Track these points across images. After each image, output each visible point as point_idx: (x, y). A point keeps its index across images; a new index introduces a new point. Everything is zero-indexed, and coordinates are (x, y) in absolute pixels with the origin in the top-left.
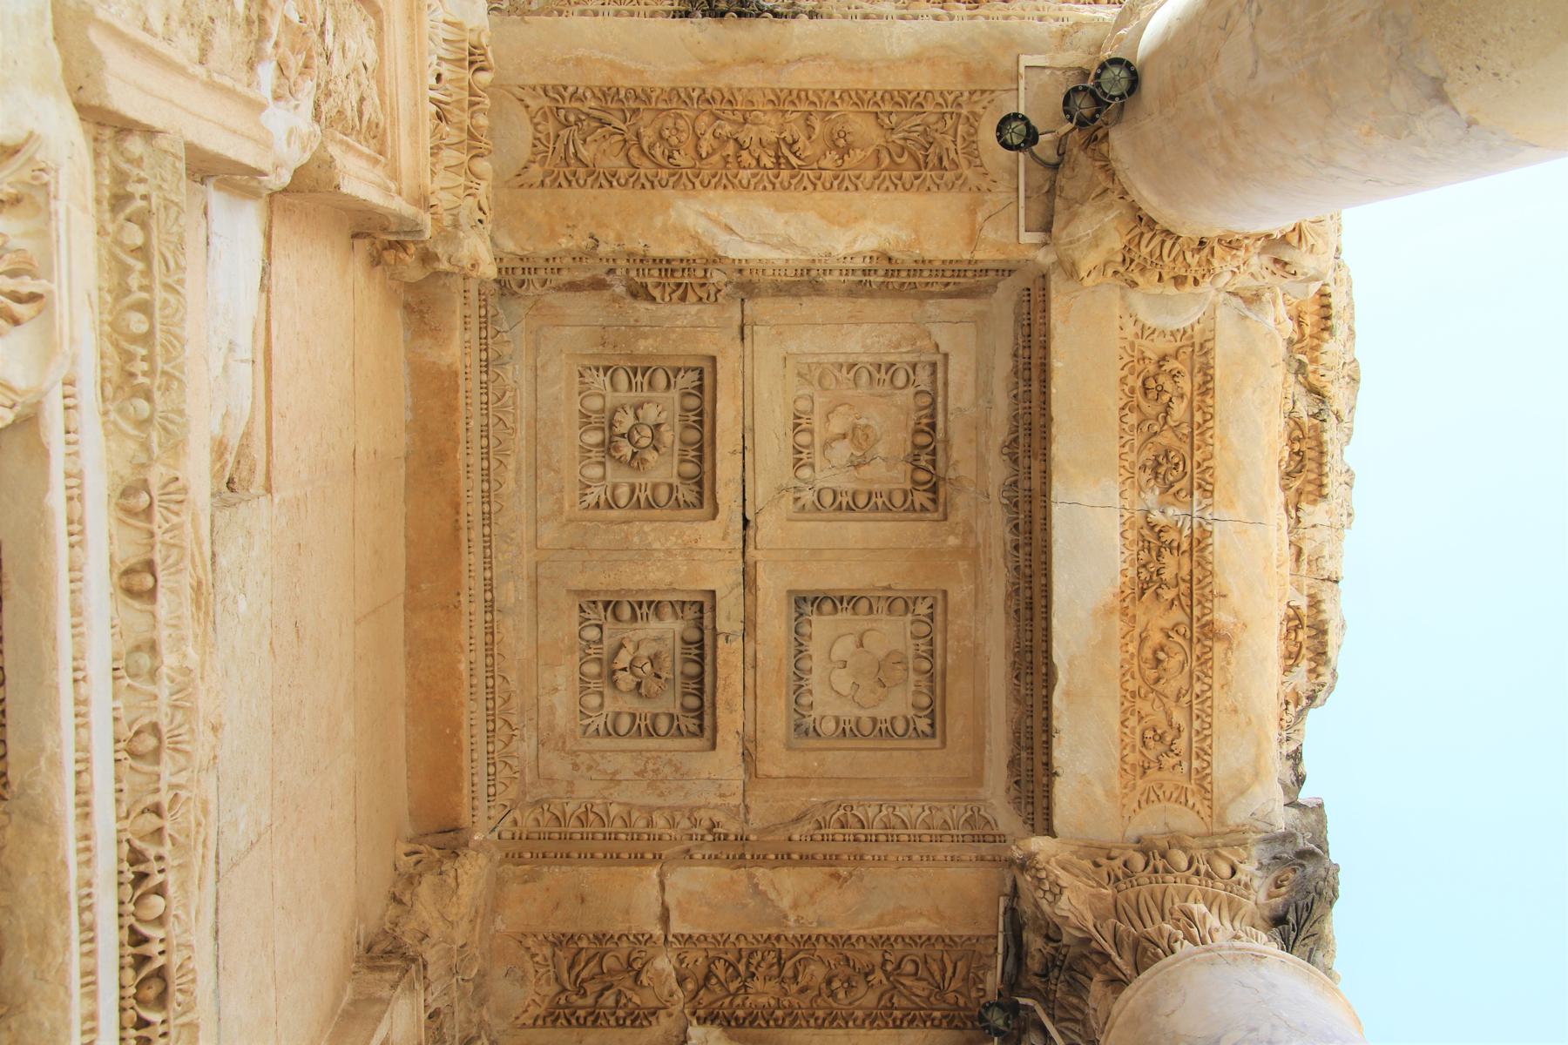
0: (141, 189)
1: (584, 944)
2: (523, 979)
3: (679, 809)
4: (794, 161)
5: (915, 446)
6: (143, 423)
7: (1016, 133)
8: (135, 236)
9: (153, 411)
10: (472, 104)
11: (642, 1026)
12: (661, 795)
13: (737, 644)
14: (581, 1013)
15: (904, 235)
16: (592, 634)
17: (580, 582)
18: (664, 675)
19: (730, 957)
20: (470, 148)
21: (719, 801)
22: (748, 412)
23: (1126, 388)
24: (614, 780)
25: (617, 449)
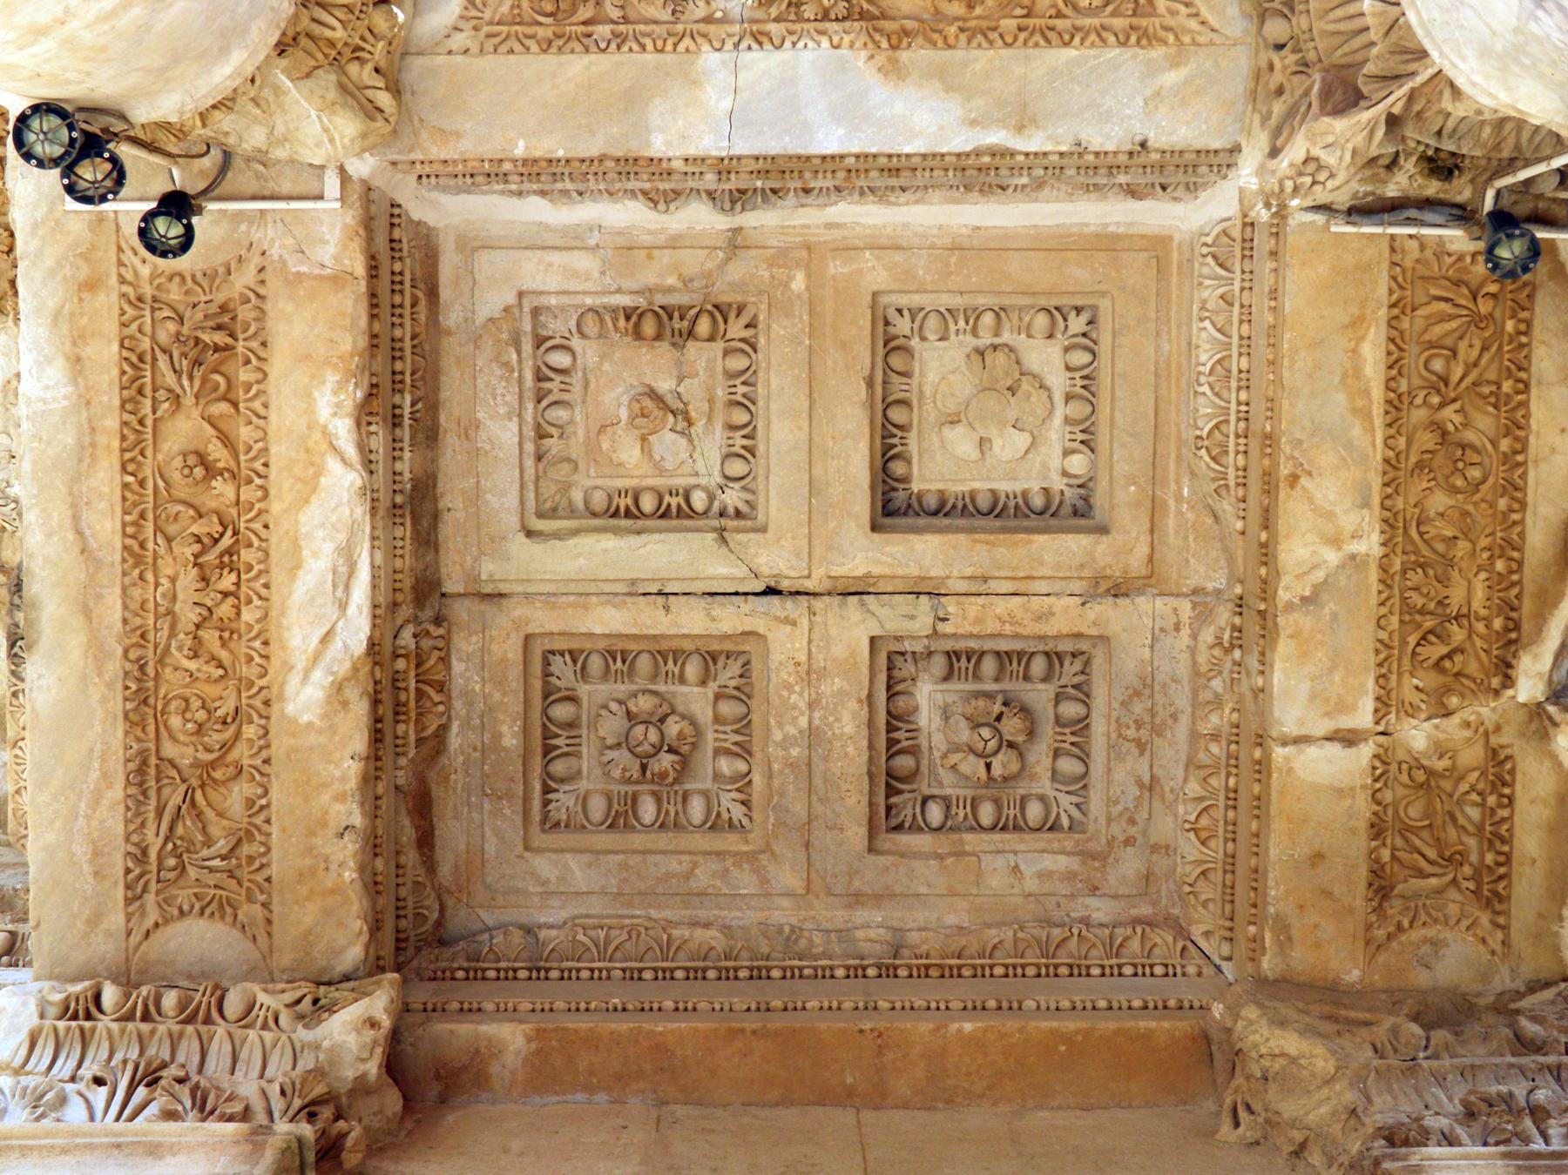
1: (1386, 855)
2: (1436, 944)
3: (1195, 693)
4: (227, 541)
5: (658, 337)
7: (167, 229)
10: (146, 1017)
11: (1512, 772)
13: (951, 605)
14: (1490, 858)
15: (332, 378)
16: (935, 813)
17: (857, 834)
19: (1412, 640)
20: (208, 1021)
21: (1185, 632)
22: (608, 588)
24: (1151, 786)
25: (663, 775)
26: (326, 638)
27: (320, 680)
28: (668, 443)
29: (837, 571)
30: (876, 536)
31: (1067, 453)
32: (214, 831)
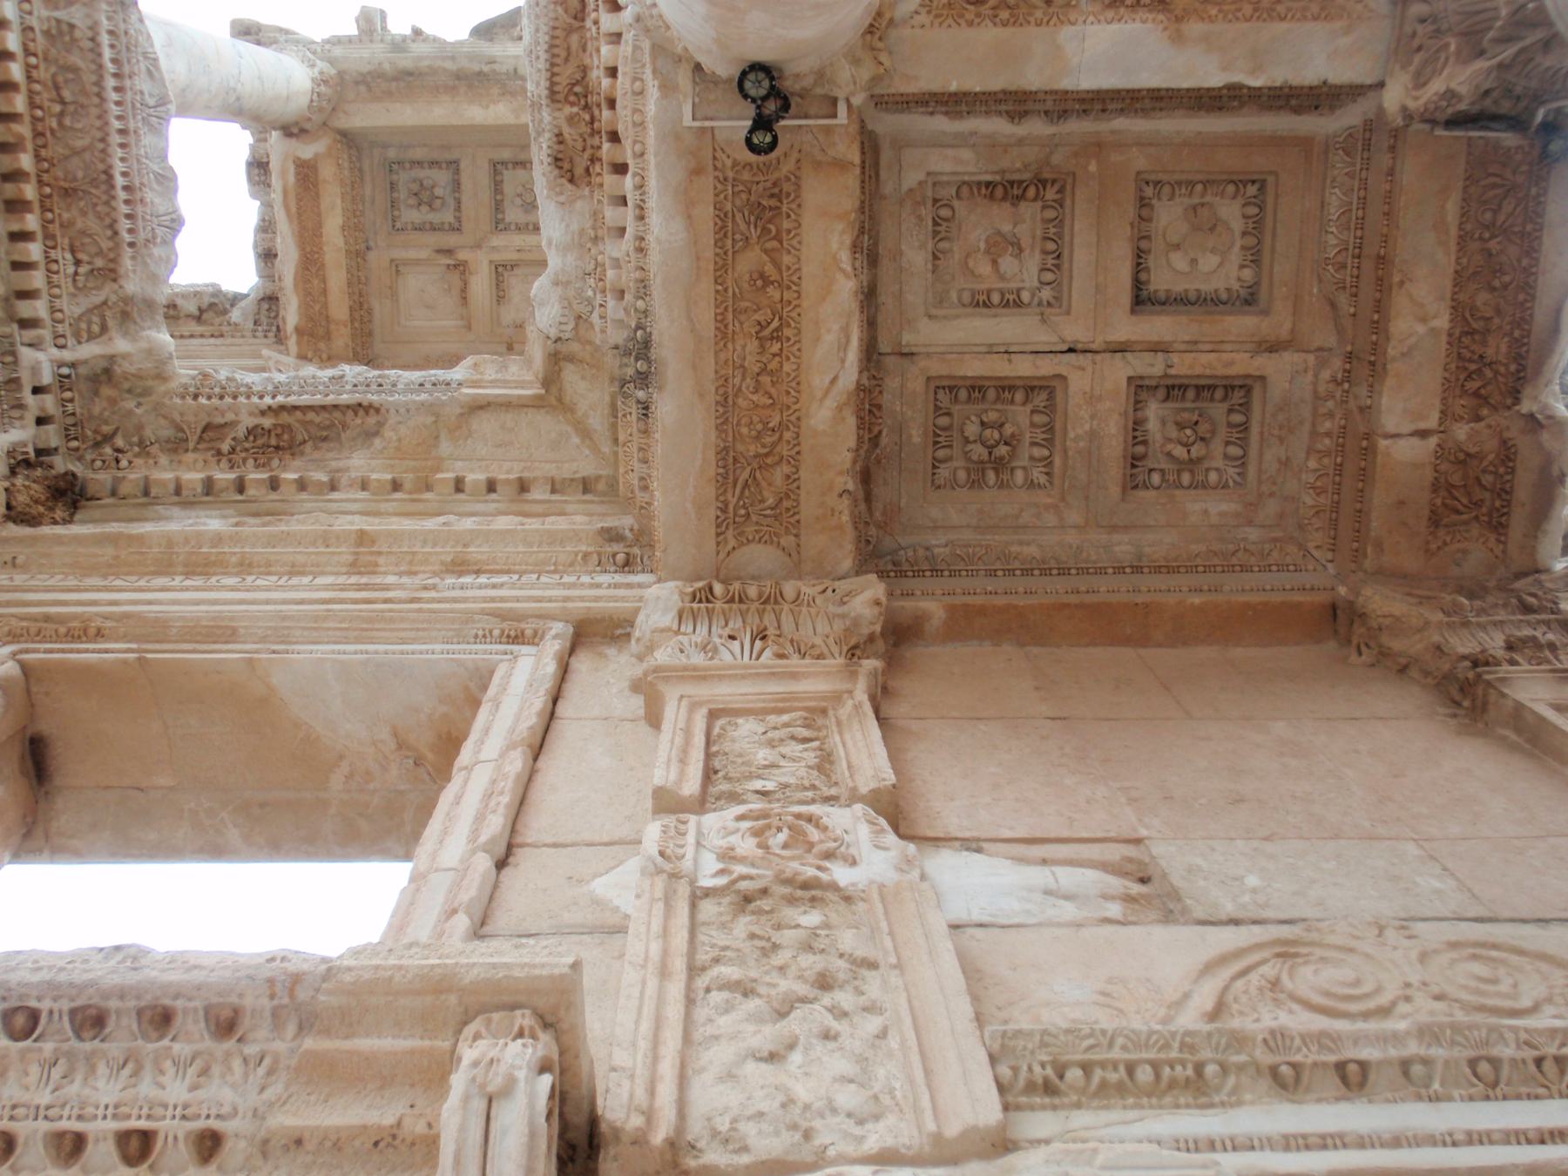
0: (1037, 1069)
1: (1439, 501)
2: (1465, 552)
3: (1315, 409)
4: (775, 324)
5: (1004, 199)
6: (1224, 1069)
7: (762, 138)
8: (1074, 1074)
9: (1213, 1061)
10: (741, 601)
11: (1515, 453)
12: (1301, 423)
13: (1175, 358)
14: (1498, 504)
15: (840, 227)
17: (1115, 491)
18: (1195, 418)
19: (1462, 377)
20: (776, 602)
21: (1311, 373)
22: (976, 349)
23: (977, 20)
25: (1002, 458)
26: (834, 381)
27: (830, 403)
28: (1008, 264)
29: (1111, 338)
30: (1134, 318)
31: (1242, 267)
32: (766, 493)
